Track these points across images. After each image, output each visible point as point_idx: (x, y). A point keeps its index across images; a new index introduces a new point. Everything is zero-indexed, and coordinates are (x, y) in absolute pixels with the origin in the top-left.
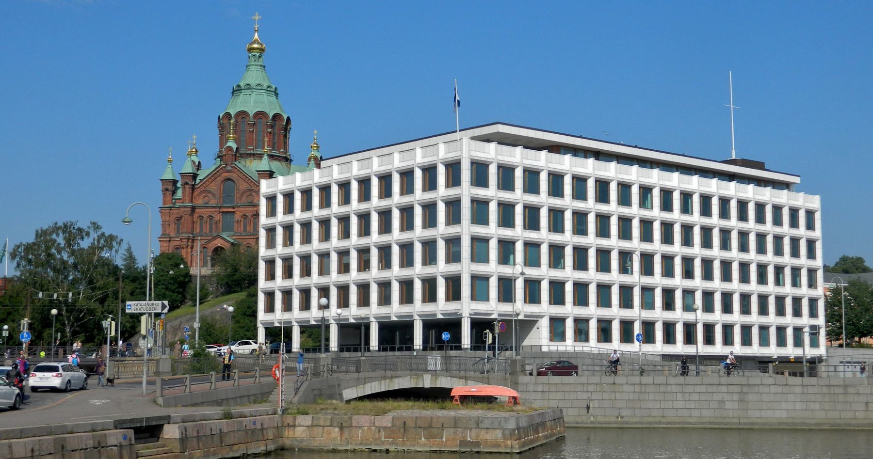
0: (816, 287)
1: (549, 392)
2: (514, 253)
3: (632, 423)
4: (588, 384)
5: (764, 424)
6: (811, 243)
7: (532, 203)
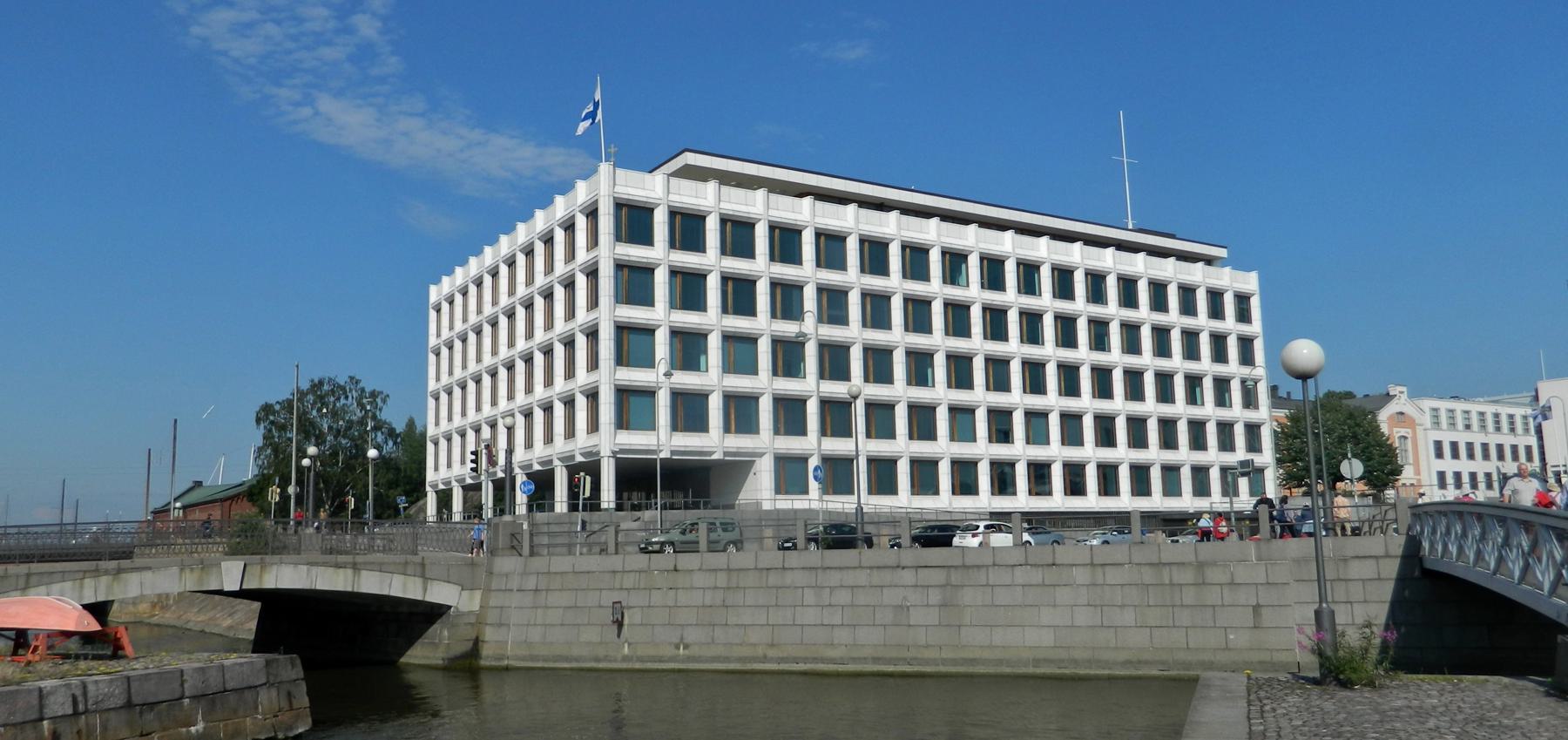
0: (1257, 407)
1: (547, 590)
2: (705, 352)
3: (708, 660)
4: (624, 572)
5: (1000, 662)
6: (1246, 343)
7: (737, 271)
